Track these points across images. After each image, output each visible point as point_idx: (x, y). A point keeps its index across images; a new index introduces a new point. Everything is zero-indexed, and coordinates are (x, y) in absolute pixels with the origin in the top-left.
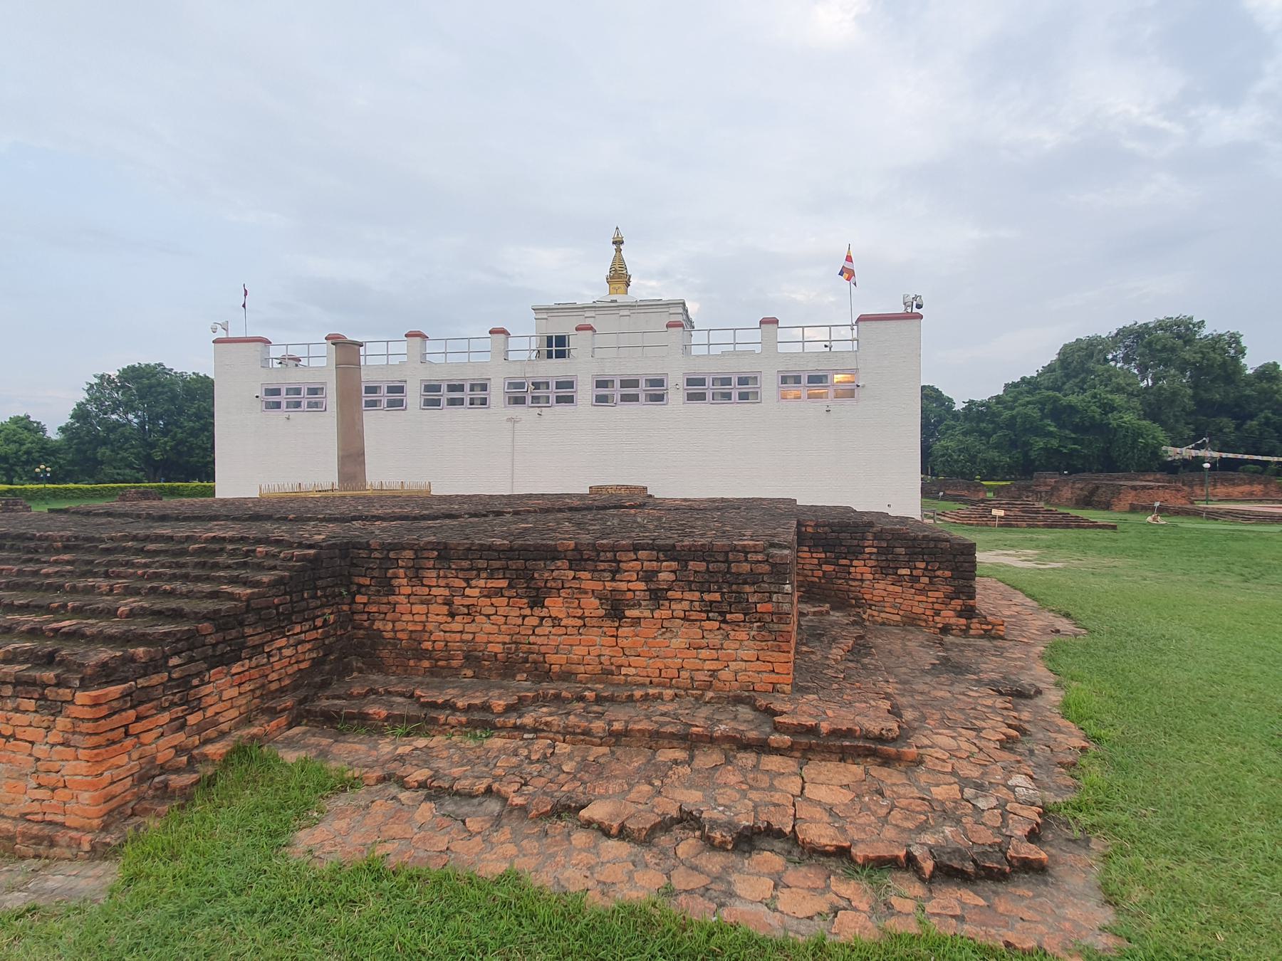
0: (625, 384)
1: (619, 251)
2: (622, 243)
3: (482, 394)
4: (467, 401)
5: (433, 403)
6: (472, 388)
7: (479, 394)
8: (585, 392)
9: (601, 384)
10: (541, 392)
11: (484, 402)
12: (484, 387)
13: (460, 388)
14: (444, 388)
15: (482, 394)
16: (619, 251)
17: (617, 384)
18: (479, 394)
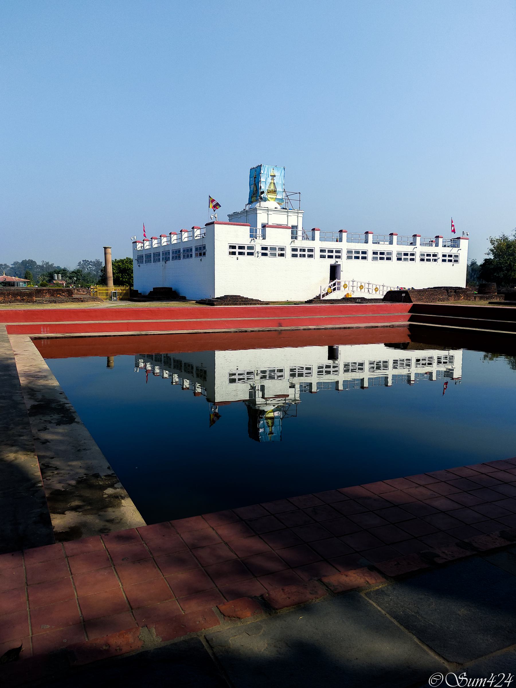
0: (329, 251)
8: (317, 253)
9: (322, 251)
11: (282, 255)
13: (274, 249)
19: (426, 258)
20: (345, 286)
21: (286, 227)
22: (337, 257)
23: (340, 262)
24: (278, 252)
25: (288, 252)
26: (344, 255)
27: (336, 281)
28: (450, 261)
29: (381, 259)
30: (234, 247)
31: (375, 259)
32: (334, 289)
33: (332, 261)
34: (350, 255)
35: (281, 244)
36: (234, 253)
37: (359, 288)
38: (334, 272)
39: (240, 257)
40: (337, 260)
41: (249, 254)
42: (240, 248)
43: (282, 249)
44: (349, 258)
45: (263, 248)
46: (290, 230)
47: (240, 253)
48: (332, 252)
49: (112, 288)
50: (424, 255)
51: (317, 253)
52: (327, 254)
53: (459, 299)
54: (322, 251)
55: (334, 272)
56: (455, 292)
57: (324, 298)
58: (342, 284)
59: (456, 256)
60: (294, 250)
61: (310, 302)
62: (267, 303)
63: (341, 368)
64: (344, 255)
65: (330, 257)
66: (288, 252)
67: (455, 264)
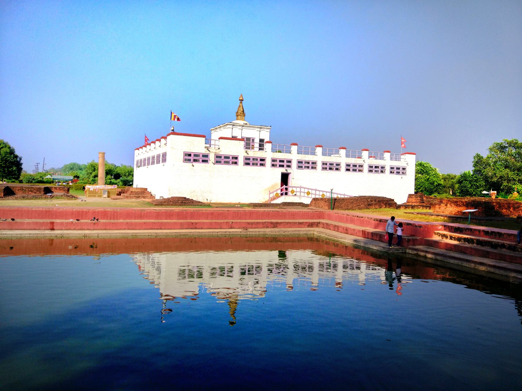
0: (280, 161)
1: (241, 103)
2: (242, 100)
3: (235, 161)
4: (231, 162)
5: (217, 162)
6: (233, 158)
7: (235, 160)
8: (268, 162)
10: (255, 162)
11: (236, 163)
12: (236, 158)
13: (228, 158)
14: (223, 157)
15: (235, 161)
16: (241, 103)
17: (278, 161)
18: (235, 160)
19: (374, 169)
20: (293, 192)
21: (242, 139)
22: (289, 166)
23: (289, 170)
24: (231, 160)
25: (241, 161)
26: (294, 164)
27: (284, 187)
28: (398, 173)
29: (330, 169)
30: (190, 155)
31: (324, 169)
32: (282, 194)
33: (283, 170)
34: (300, 165)
35: (235, 154)
36: (189, 160)
37: (306, 194)
38: (285, 178)
39: (195, 164)
40: (288, 169)
41: (203, 161)
42: (196, 155)
43: (236, 158)
44: (300, 167)
45: (218, 157)
46: (242, 143)
47: (195, 161)
48: (283, 161)
49: (100, 186)
50: (372, 167)
51: (268, 162)
52: (278, 163)
53: (381, 208)
54: (273, 160)
55: (285, 178)
56: (375, 201)
57: (272, 202)
58: (290, 189)
59: (404, 169)
60: (247, 159)
61: (250, 205)
62: (209, 205)
63: (291, 266)
64: (294, 164)
65: (280, 166)
66: (241, 161)
67: (403, 176)
